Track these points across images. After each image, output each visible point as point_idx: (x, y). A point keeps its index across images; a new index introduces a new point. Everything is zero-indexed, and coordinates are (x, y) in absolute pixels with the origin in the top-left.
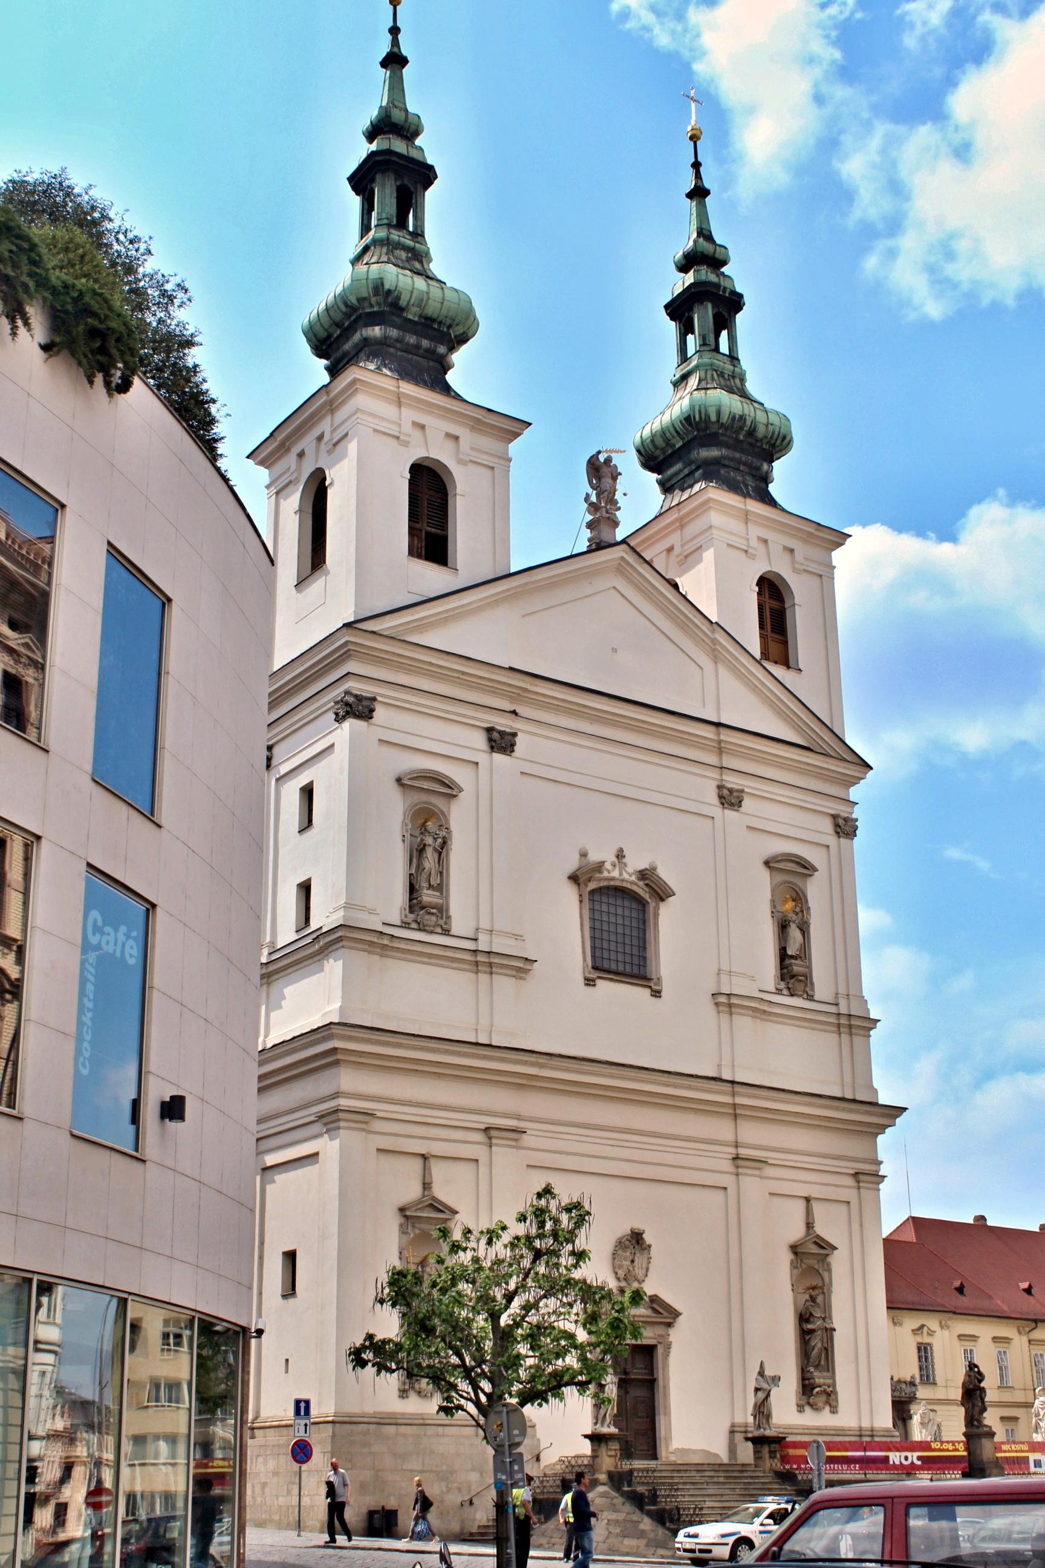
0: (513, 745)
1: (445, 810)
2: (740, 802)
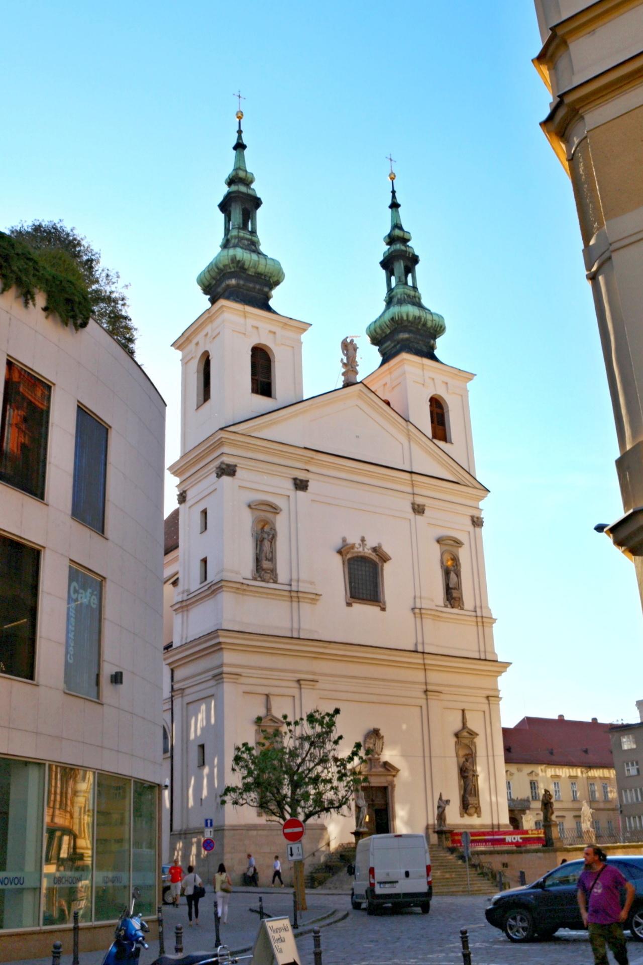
1: (273, 520)
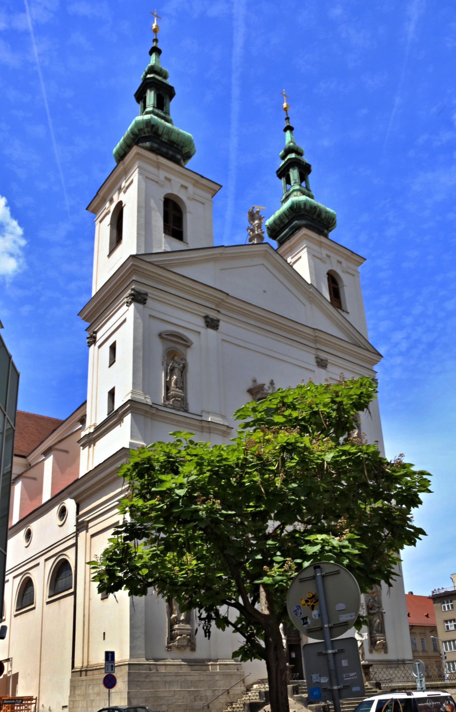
0: (218, 326)
2: (326, 365)
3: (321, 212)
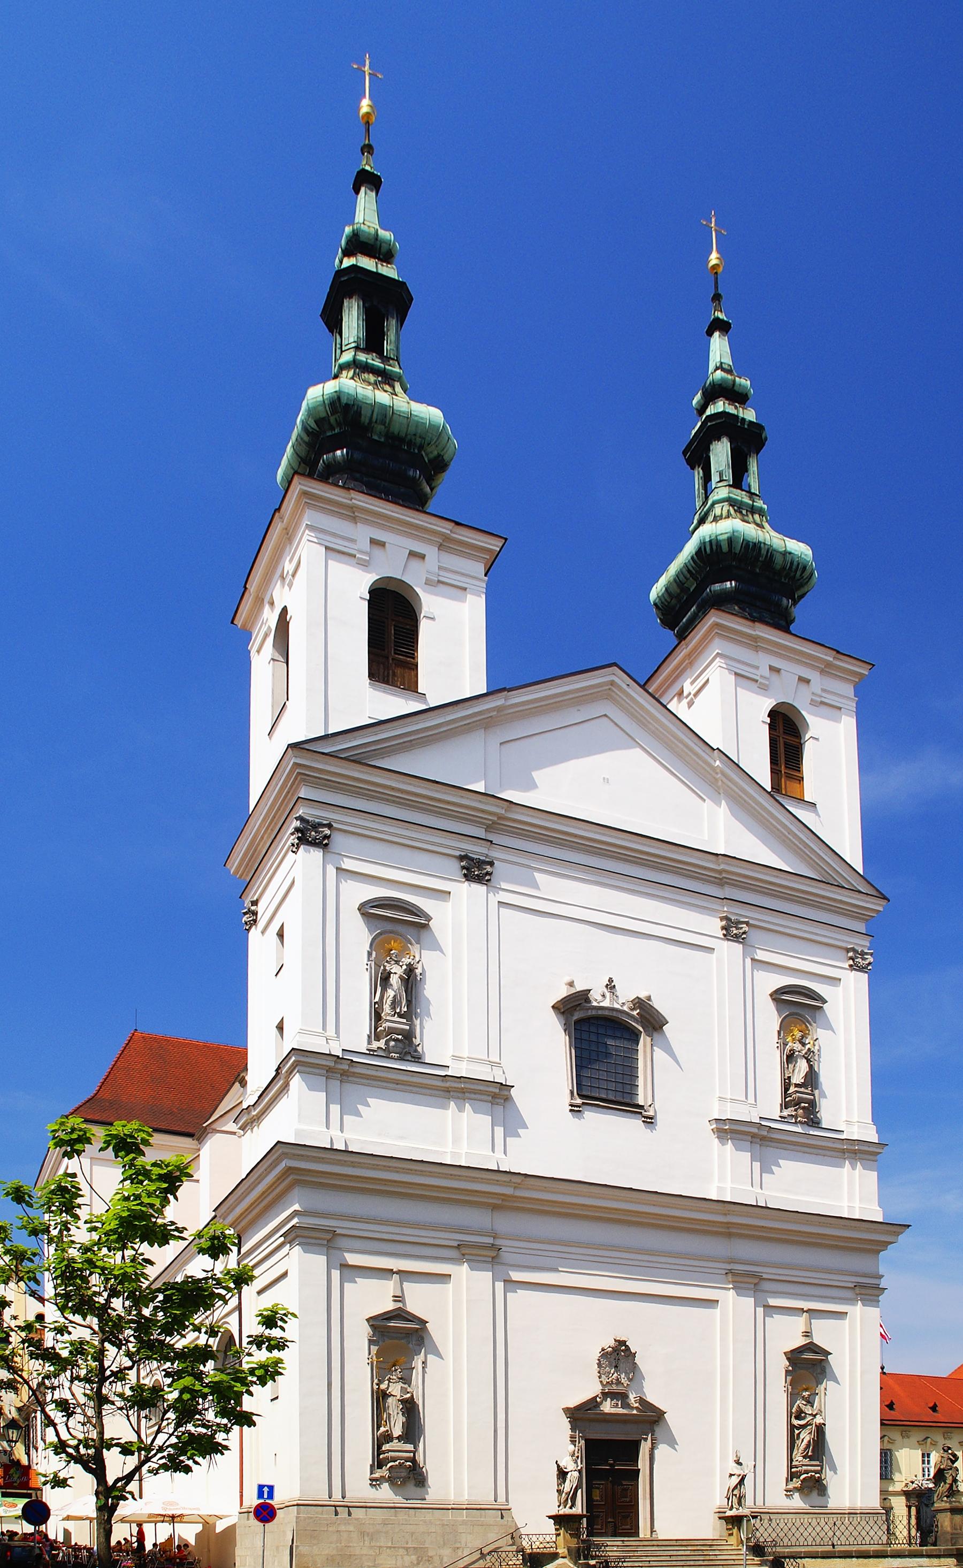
3: (772, 555)
